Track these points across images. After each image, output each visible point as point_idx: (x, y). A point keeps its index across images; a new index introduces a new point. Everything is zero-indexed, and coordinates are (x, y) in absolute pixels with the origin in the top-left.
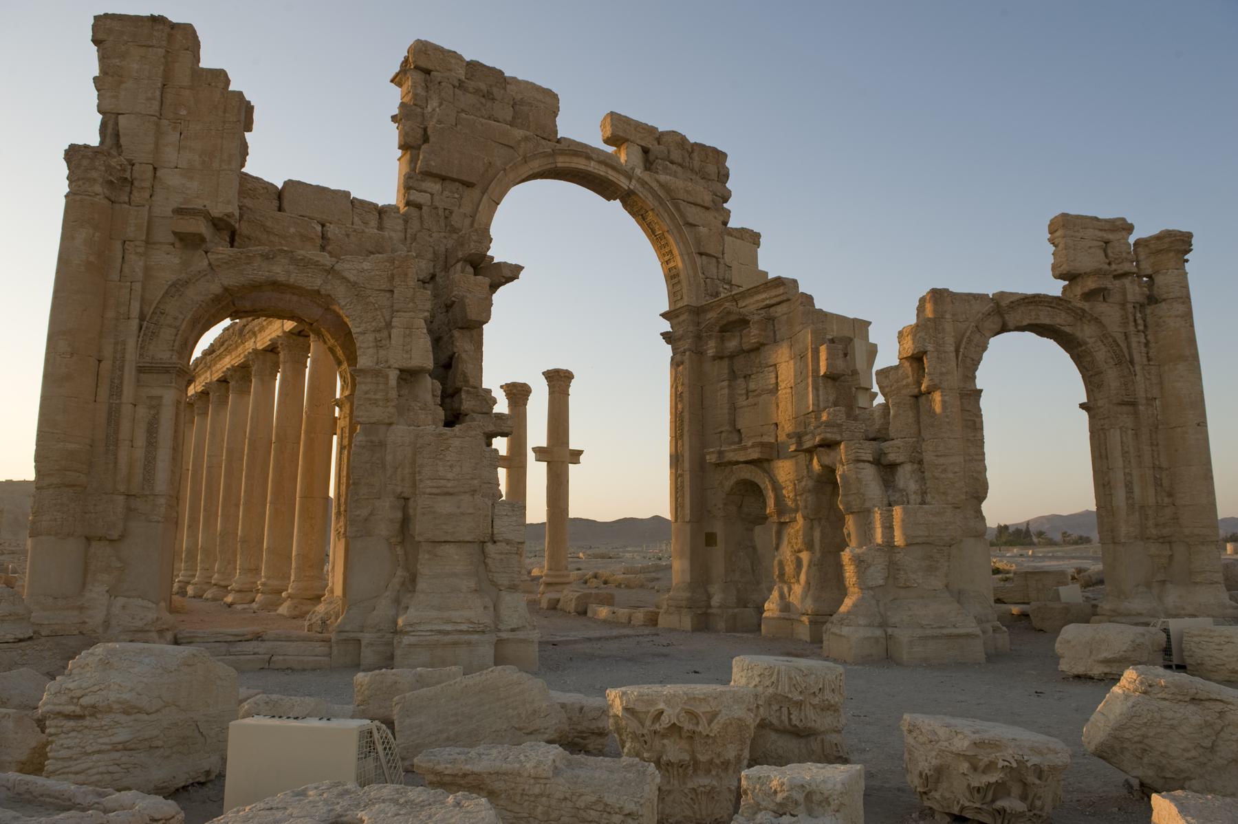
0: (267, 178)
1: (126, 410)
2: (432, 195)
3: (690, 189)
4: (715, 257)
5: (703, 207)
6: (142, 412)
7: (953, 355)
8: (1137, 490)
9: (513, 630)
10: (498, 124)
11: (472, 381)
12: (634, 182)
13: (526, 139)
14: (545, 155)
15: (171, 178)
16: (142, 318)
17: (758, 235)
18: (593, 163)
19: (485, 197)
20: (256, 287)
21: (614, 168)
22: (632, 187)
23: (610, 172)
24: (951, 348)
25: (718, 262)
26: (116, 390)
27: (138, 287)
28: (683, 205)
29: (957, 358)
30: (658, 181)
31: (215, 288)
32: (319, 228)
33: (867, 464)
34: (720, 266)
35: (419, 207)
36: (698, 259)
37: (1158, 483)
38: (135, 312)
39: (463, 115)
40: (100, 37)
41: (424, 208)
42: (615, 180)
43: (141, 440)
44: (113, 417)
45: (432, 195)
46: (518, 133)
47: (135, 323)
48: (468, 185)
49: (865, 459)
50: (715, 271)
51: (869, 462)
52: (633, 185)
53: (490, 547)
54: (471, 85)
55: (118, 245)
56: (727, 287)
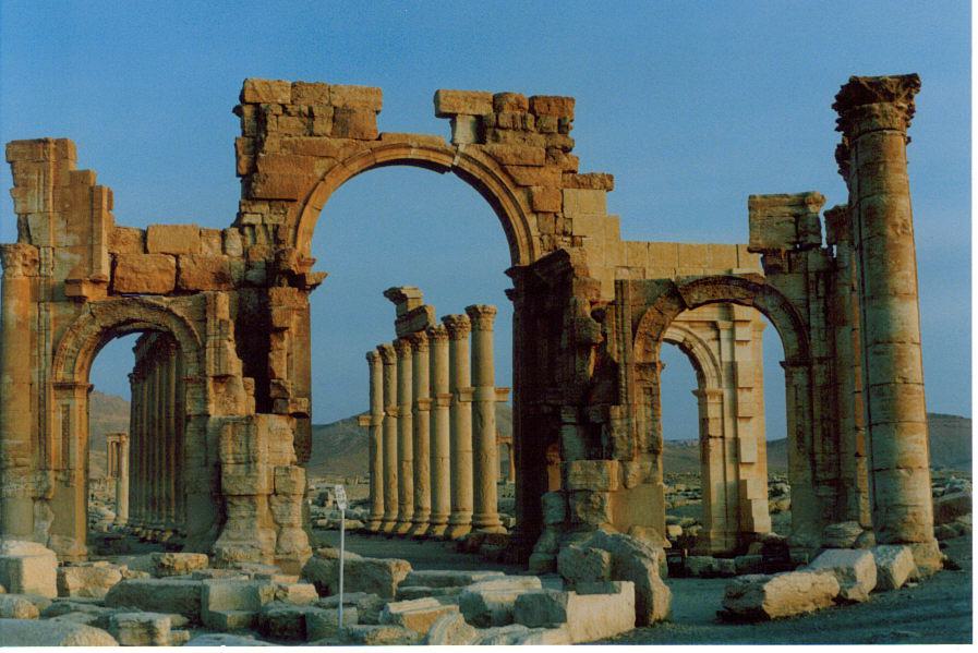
2: (262, 214)
3: (519, 152)
8: (807, 439)
11: (277, 374)
12: (457, 158)
14: (363, 156)
16: (54, 353)
18: (413, 151)
20: (120, 324)
22: (455, 164)
28: (513, 170)
30: (484, 152)
31: (96, 328)
36: (532, 220)
37: (825, 434)
39: (287, 138)
40: (11, 159)
41: (257, 227)
42: (438, 161)
46: (337, 143)
47: (50, 357)
50: (552, 226)
52: (457, 161)
56: (568, 239)
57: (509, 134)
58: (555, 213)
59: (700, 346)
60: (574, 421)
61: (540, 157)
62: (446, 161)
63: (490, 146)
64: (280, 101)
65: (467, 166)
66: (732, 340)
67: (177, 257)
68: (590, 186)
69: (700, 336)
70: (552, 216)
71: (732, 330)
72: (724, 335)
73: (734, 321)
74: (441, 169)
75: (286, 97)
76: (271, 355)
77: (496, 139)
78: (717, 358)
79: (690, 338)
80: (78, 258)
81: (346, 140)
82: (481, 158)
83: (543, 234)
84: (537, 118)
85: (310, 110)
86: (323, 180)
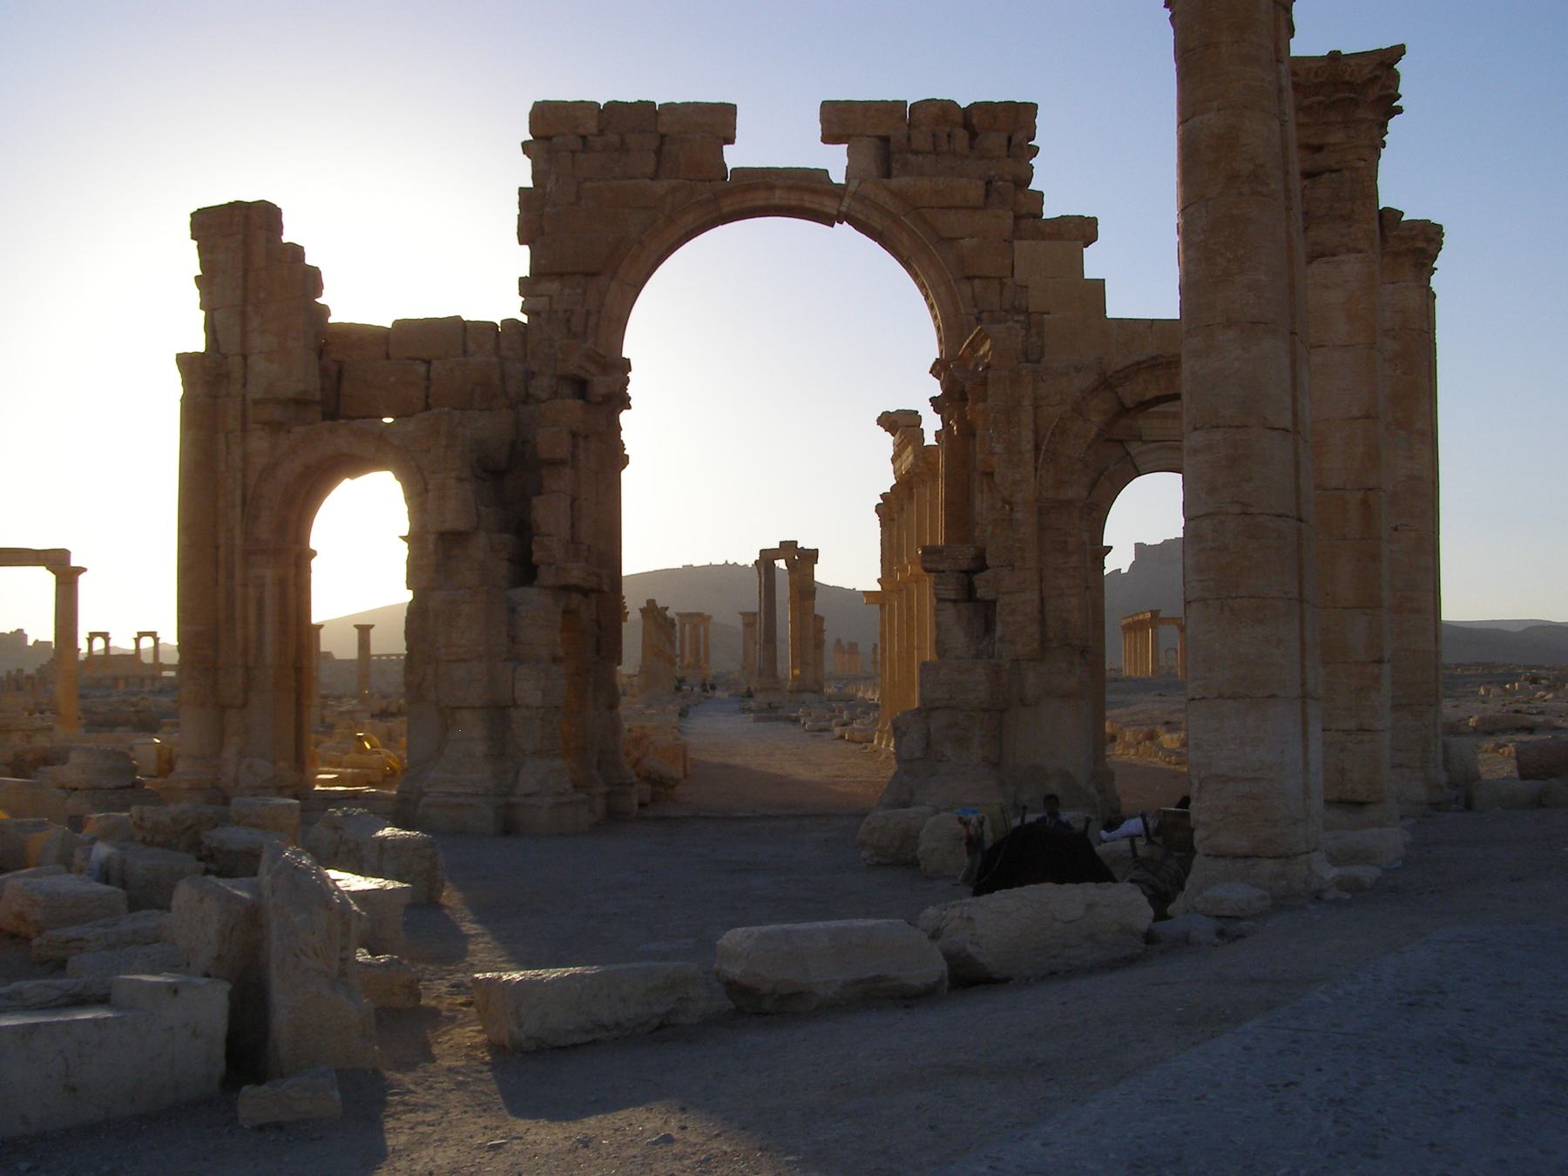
2: (551, 297)
4: (995, 278)
5: (967, 208)
7: (1029, 456)
9: (527, 795)
10: (633, 181)
15: (259, 364)
17: (1095, 219)
18: (778, 193)
21: (814, 191)
23: (806, 197)
24: (1027, 446)
25: (1002, 284)
29: (1036, 461)
32: (422, 369)
33: (948, 604)
38: (238, 502)
39: (588, 184)
43: (252, 619)
45: (551, 297)
46: (661, 186)
47: (238, 509)
48: (593, 275)
49: (946, 597)
56: (1022, 318)
58: (1001, 279)
60: (953, 597)
62: (830, 206)
63: (894, 183)
64: (581, 131)
67: (428, 362)
75: (591, 126)
76: (535, 501)
83: (981, 312)
84: (973, 136)
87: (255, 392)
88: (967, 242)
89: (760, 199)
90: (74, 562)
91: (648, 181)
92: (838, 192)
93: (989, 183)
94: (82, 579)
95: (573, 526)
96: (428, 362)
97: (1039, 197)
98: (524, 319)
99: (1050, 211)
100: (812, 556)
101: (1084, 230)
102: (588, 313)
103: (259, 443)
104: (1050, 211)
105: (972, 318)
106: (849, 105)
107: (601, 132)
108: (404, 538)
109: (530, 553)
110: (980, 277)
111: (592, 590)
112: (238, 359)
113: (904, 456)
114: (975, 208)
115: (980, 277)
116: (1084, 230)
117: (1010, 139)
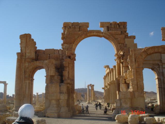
0: (43, 49)
1: (23, 84)
6: (25, 84)
7: (134, 62)
9: (62, 112)
12: (103, 34)
13: (81, 33)
15: (27, 54)
18: (95, 33)
19: (74, 45)
21: (99, 33)
23: (98, 34)
24: (134, 60)
26: (22, 82)
27: (24, 68)
29: (135, 62)
32: (49, 55)
34: (124, 45)
35: (64, 48)
36: (119, 45)
44: (22, 85)
46: (80, 32)
48: (71, 43)
51: (123, 83)
53: (60, 101)
54: (72, 27)
55: (22, 64)
57: (114, 29)
59: (155, 69)
60: (123, 83)
61: (120, 32)
62: (101, 35)
64: (70, 26)
65: (105, 35)
66: (162, 67)
67: (50, 55)
68: (131, 38)
69: (155, 67)
70: (123, 44)
71: (162, 65)
72: (161, 66)
73: (163, 63)
74: (101, 36)
75: (71, 25)
77: (111, 30)
78: (159, 71)
79: (153, 67)
80: (29, 54)
81: (81, 32)
82: (108, 33)
84: (119, 26)
85: (75, 27)
86: (77, 39)
87: (27, 57)
88: (119, 39)
89: (92, 34)
90: (7, 83)
91: (78, 32)
92: (102, 33)
93: (121, 32)
94: (8, 85)
95: (68, 75)
96: (50, 55)
97: (128, 33)
98: (62, 49)
99: (129, 35)
100: (93, 86)
101: (134, 37)
102: (70, 48)
103: (27, 64)
104: (129, 35)
105: (120, 49)
106: (103, 23)
107: (72, 26)
108: (45, 76)
109: (63, 79)
110: (121, 43)
111: (71, 84)
112: (25, 54)
113: (108, 70)
114: (120, 35)
115: (121, 43)
116: (134, 37)
117: (124, 26)
